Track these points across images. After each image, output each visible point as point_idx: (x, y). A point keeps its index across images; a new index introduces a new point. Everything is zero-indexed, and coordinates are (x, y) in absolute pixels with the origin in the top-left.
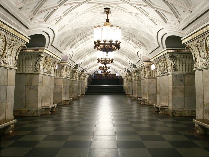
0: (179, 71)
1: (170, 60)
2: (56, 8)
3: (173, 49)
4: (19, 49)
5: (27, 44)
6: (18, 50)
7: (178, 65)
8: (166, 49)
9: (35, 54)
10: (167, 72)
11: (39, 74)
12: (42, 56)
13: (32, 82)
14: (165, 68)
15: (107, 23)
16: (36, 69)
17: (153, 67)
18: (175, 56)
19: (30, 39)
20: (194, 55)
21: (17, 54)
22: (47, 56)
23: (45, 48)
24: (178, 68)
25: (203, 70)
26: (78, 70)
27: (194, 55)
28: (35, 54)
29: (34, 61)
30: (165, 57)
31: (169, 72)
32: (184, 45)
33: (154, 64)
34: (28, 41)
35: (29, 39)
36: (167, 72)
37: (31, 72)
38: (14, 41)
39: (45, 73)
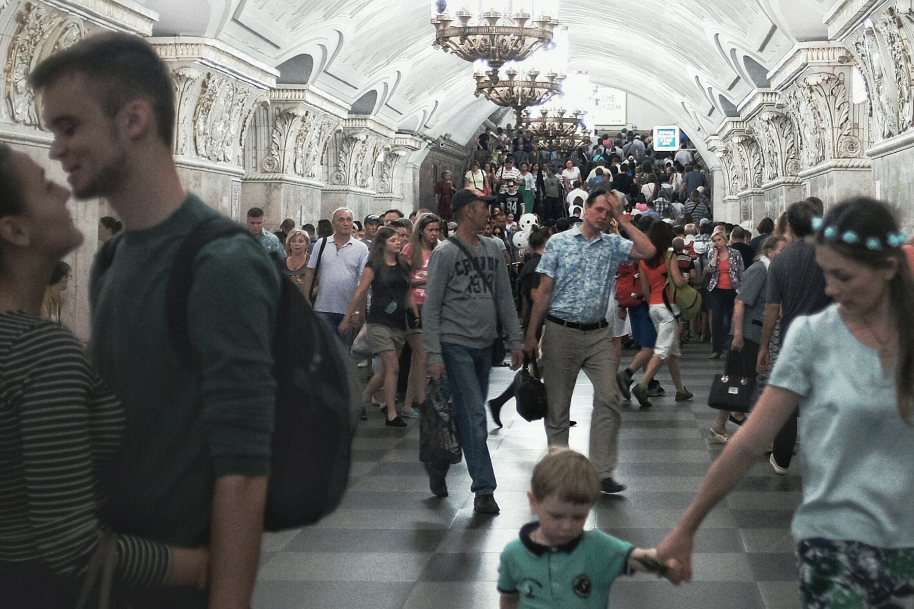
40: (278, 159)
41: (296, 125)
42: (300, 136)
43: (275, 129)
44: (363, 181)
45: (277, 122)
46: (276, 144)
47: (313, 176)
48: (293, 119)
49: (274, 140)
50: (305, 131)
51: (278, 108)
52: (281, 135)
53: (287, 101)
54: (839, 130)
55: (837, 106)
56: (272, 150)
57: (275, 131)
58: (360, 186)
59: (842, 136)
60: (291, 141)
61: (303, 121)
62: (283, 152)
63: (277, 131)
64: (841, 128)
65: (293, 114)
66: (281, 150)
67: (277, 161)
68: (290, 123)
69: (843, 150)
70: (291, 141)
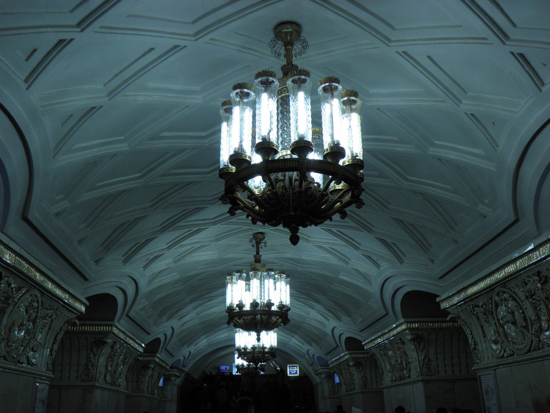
0: (438, 371)
1: (413, 347)
5: (81, 316)
11: (94, 387)
12: (107, 343)
20: (471, 334)
25: (495, 370)
27: (471, 334)
30: (401, 339)
32: (445, 313)
40: (93, 372)
41: (106, 350)
42: (111, 357)
43: (92, 351)
44: (152, 391)
45: (93, 347)
46: (92, 362)
47: (119, 385)
48: (104, 345)
49: (91, 359)
50: (114, 355)
51: (94, 337)
52: (95, 356)
53: (100, 333)
56: (89, 366)
57: (92, 353)
58: (151, 394)
59: (425, 365)
60: (102, 360)
61: (112, 347)
62: (96, 367)
63: (93, 353)
65: (104, 341)
66: (95, 366)
67: (92, 373)
68: (102, 348)
69: (425, 372)
70: (102, 360)
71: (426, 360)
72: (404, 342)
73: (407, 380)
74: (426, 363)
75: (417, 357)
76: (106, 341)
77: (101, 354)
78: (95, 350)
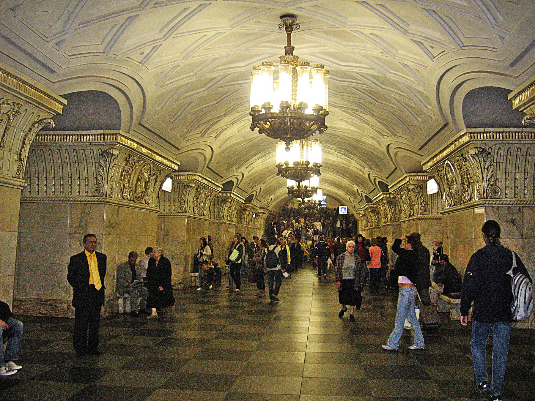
0: (506, 194)
1: (477, 164)
2: (137, 13)
3: (487, 130)
4: (30, 129)
6: (29, 131)
7: (501, 176)
8: (465, 131)
9: (94, 148)
10: (470, 200)
13: (86, 225)
14: (464, 188)
15: (289, 57)
16: (96, 190)
17: (432, 187)
18: (494, 150)
19: (65, 102)
21: (24, 143)
22: (129, 155)
23: (121, 132)
24: (501, 184)
26: (232, 195)
28: (94, 148)
29: (92, 167)
31: (476, 199)
33: (434, 177)
34: (60, 109)
35: (61, 103)
36: (470, 200)
37: (84, 196)
38: (8, 104)
39: (126, 202)
43: (100, 165)
46: (101, 176)
49: (100, 173)
54: (487, 182)
55: (486, 167)
56: (99, 180)
59: (490, 186)
63: (101, 166)
64: (488, 181)
71: (492, 181)
72: (466, 158)
73: (468, 204)
74: (492, 183)
75: (481, 176)
76: (111, 153)
77: (111, 167)
78: (102, 163)
